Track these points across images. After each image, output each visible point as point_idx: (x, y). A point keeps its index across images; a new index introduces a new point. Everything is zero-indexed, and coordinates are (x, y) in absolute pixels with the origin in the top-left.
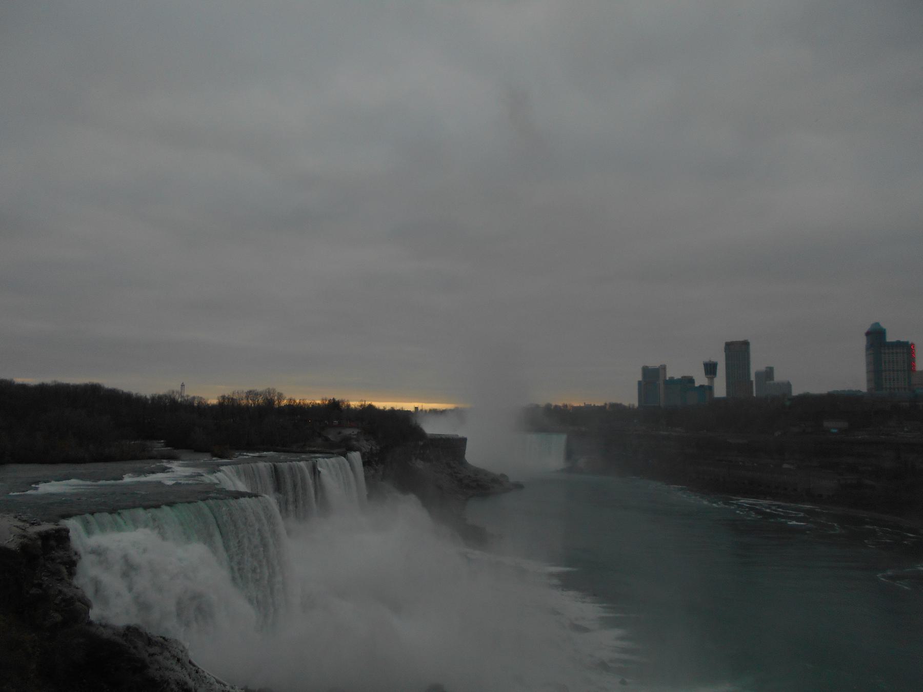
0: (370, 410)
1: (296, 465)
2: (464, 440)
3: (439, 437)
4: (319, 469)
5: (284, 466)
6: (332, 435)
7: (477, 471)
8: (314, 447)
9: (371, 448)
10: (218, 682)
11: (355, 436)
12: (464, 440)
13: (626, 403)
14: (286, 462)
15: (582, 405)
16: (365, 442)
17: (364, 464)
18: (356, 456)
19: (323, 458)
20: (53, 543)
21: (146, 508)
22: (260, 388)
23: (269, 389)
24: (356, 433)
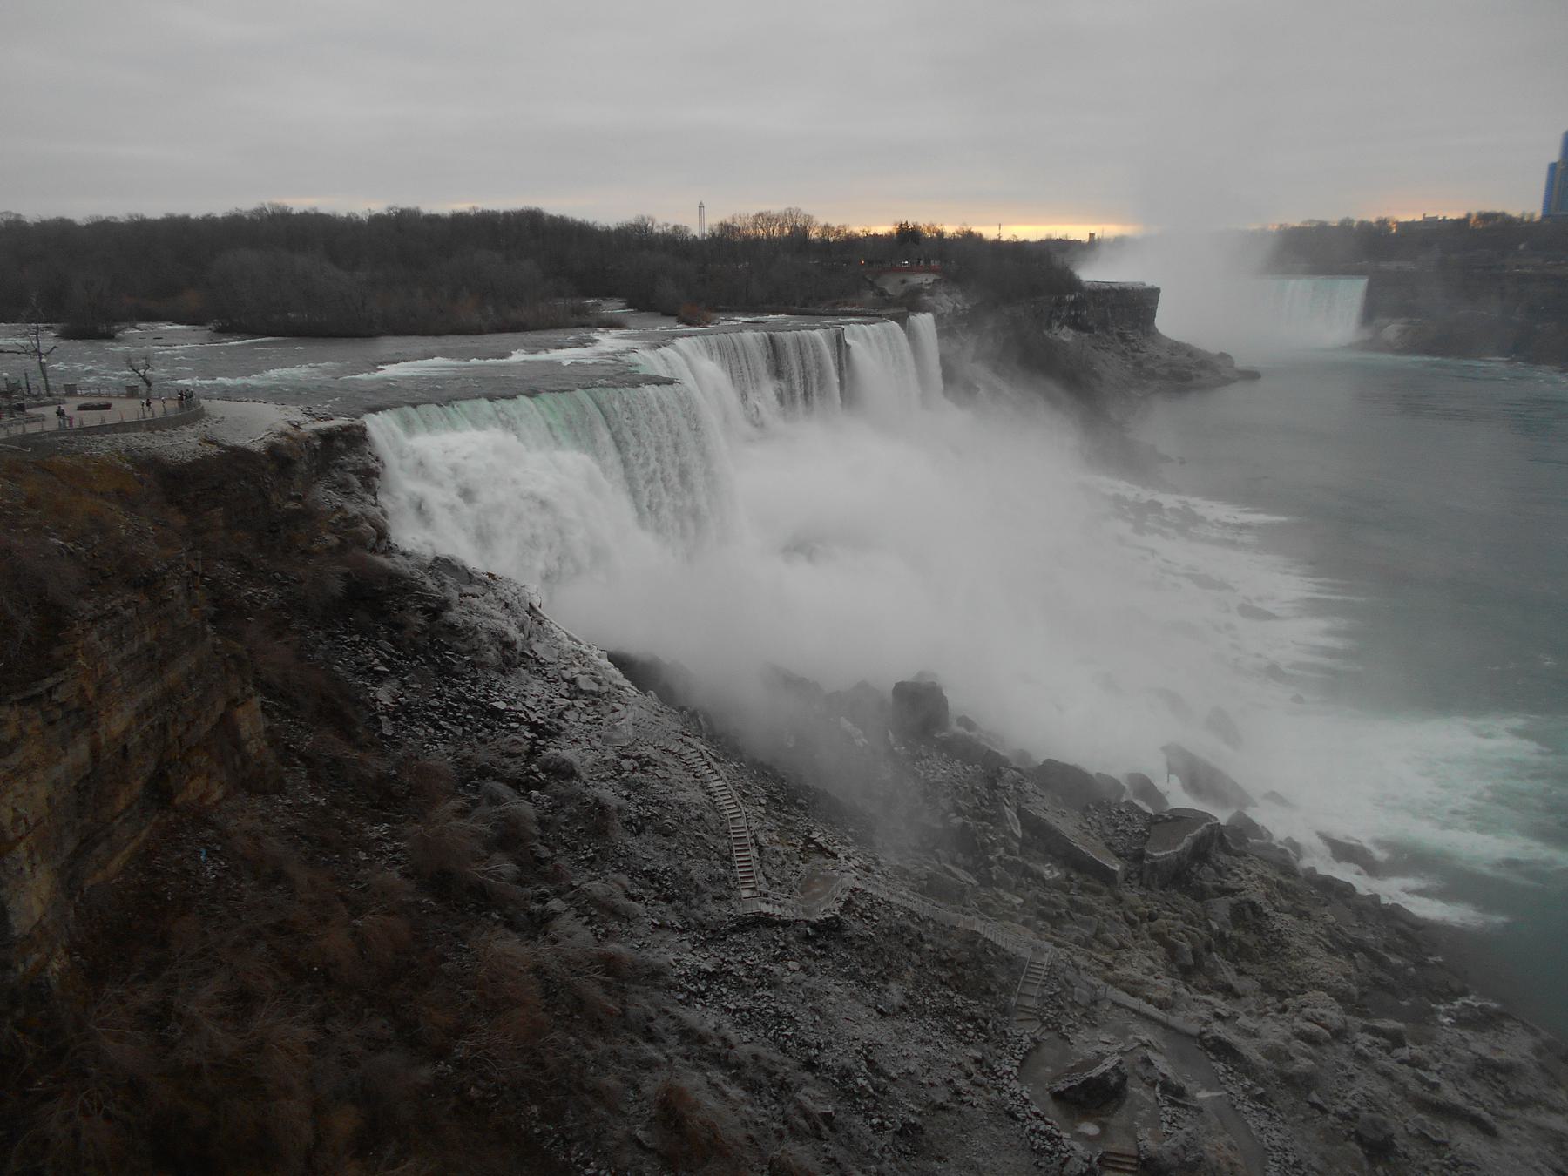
0: (970, 241)
1: (808, 341)
2: (1155, 292)
3: (1107, 287)
4: (849, 341)
5: (787, 337)
6: (892, 285)
7: (1177, 347)
8: (853, 305)
9: (955, 307)
10: (570, 638)
11: (928, 288)
12: (1155, 292)
13: (1515, 211)
14: (790, 331)
15: (1419, 218)
16: (945, 296)
17: (942, 333)
18: (924, 322)
19: (859, 323)
20: (339, 444)
21: (491, 398)
22: (775, 208)
23: (790, 209)
24: (930, 281)
